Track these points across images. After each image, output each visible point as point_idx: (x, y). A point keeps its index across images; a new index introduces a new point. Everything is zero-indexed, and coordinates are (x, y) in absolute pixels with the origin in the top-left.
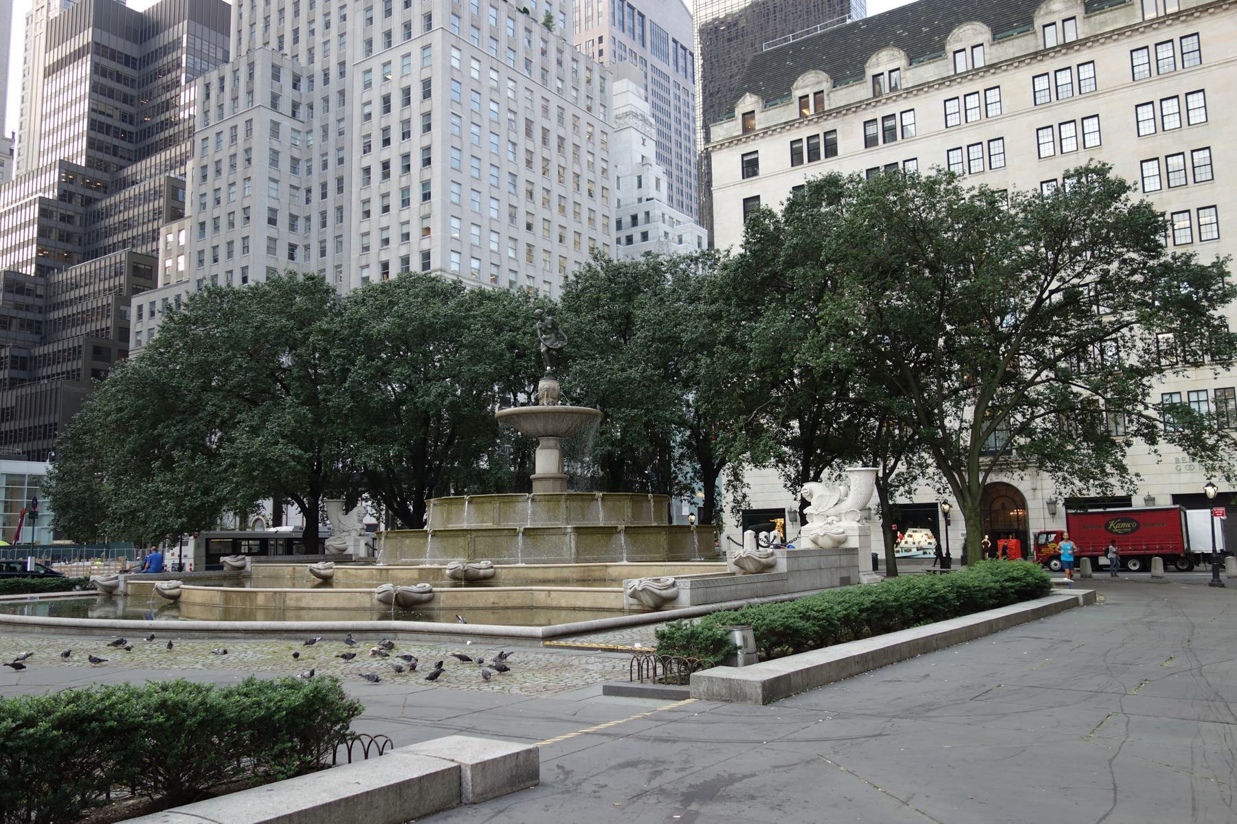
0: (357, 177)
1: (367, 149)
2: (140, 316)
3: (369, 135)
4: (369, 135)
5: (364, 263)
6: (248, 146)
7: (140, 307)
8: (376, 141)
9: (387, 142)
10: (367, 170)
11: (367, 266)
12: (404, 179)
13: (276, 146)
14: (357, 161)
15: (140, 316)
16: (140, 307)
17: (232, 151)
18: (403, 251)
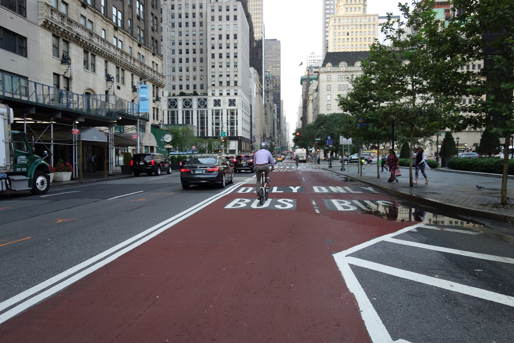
14: (210, 51)
18: (228, 79)
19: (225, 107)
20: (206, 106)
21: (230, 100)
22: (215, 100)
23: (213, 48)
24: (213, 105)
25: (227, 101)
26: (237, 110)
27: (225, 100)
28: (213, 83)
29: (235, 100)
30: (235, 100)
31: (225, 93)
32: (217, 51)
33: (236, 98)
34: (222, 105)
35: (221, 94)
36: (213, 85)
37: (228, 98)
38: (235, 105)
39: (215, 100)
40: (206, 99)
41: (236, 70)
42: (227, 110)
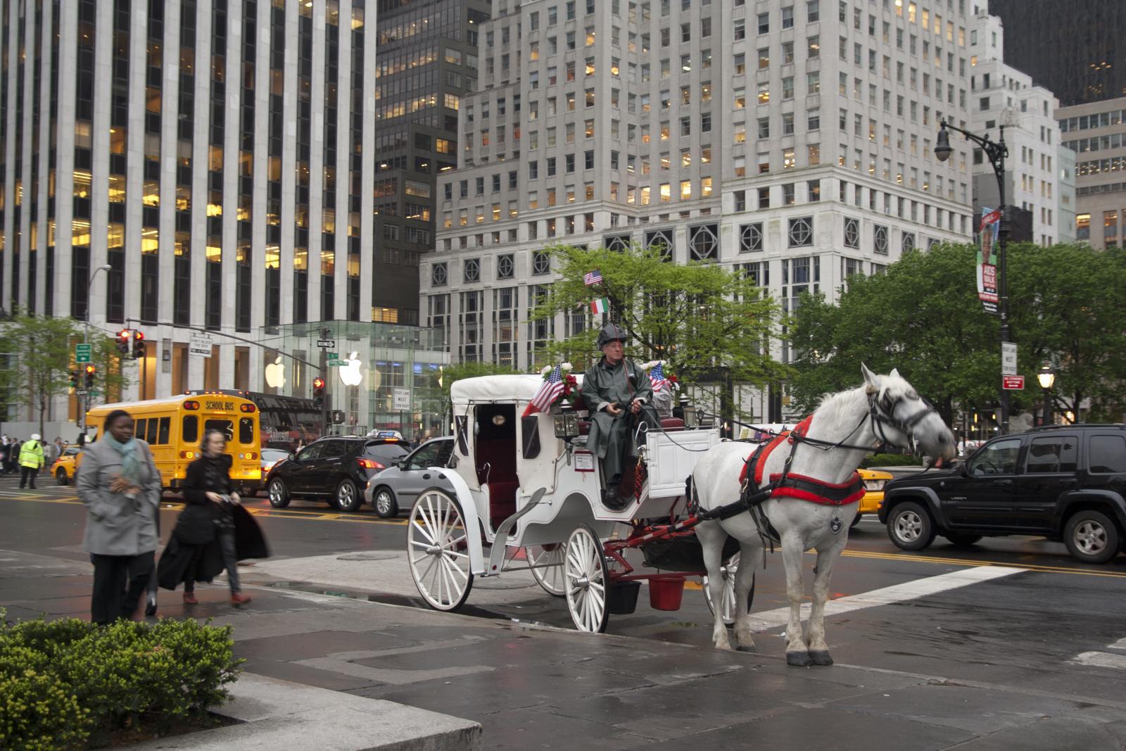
0: (728, 65)
1: (741, 34)
2: (449, 196)
3: (743, 21)
4: (743, 21)
5: (738, 154)
6: (589, 24)
7: (448, 187)
8: (751, 27)
9: (764, 29)
10: (740, 57)
11: (743, 157)
12: (786, 69)
13: (618, 25)
14: (728, 46)
15: (449, 196)
16: (448, 187)
17: (570, 28)
19: (776, 248)
20: (714, 254)
21: (792, 222)
22: (743, 228)
23: (741, 34)
24: (736, 247)
25: (784, 228)
26: (817, 259)
27: (775, 224)
28: (739, 164)
29: (809, 220)
30: (809, 220)
31: (776, 196)
32: (750, 45)
33: (815, 211)
34: (765, 244)
35: (764, 202)
36: (741, 172)
37: (784, 217)
38: (809, 241)
39: (743, 228)
40: (714, 228)
41: (815, 104)
42: (785, 262)
